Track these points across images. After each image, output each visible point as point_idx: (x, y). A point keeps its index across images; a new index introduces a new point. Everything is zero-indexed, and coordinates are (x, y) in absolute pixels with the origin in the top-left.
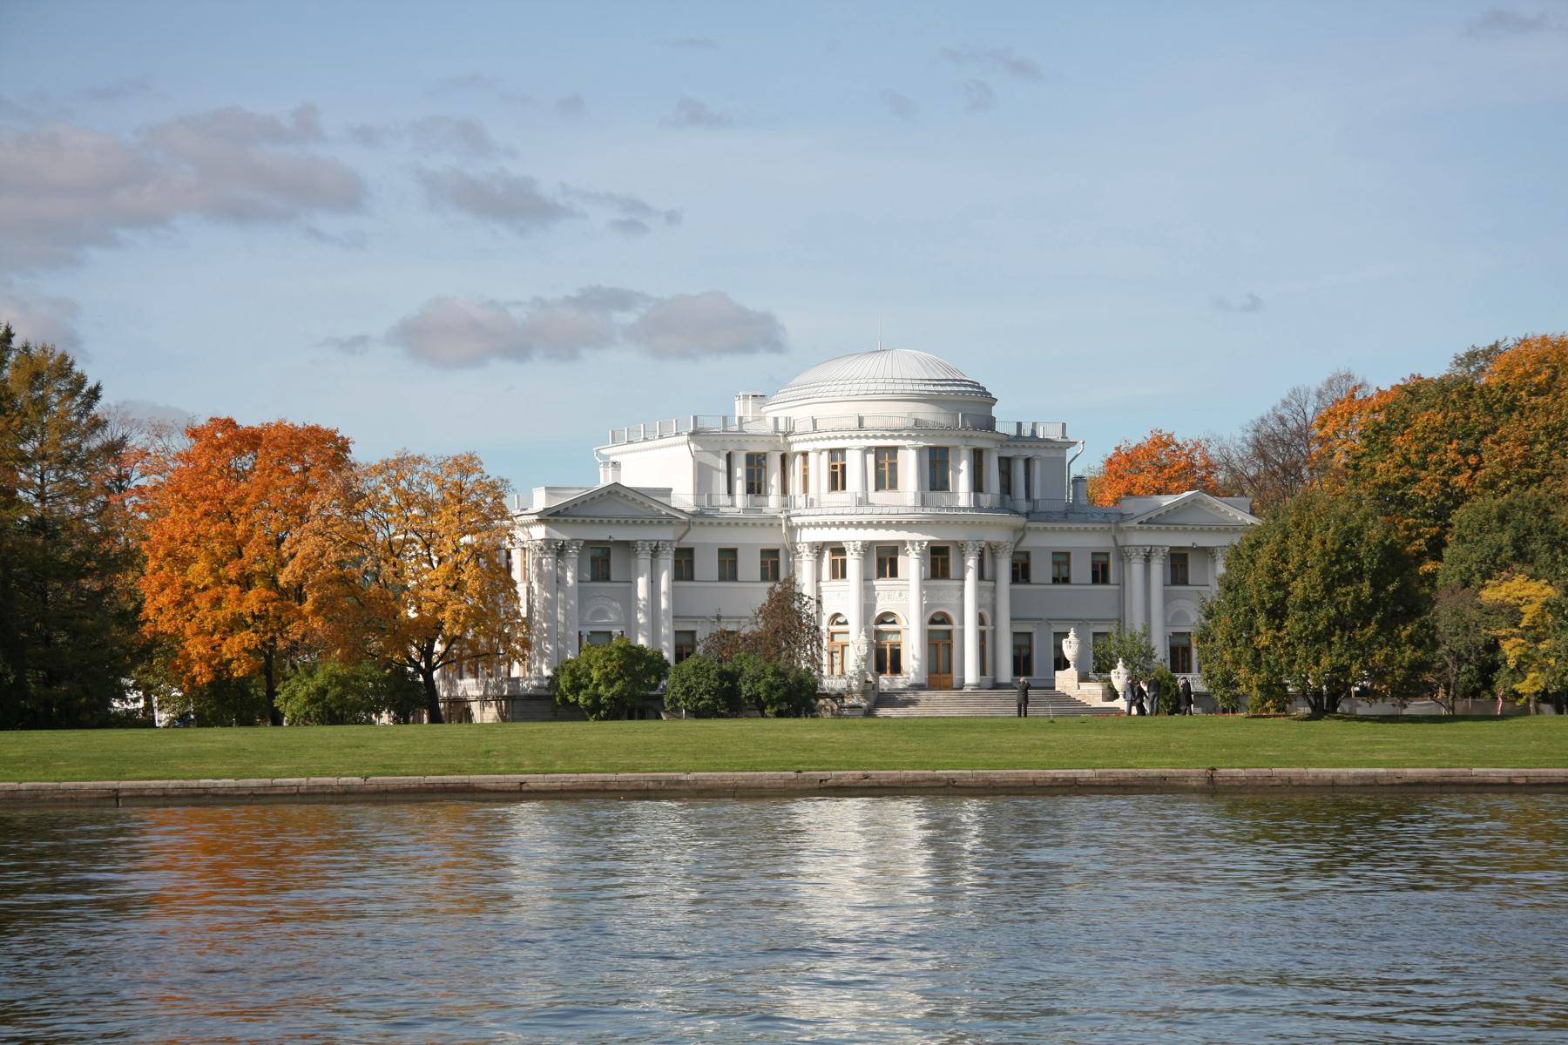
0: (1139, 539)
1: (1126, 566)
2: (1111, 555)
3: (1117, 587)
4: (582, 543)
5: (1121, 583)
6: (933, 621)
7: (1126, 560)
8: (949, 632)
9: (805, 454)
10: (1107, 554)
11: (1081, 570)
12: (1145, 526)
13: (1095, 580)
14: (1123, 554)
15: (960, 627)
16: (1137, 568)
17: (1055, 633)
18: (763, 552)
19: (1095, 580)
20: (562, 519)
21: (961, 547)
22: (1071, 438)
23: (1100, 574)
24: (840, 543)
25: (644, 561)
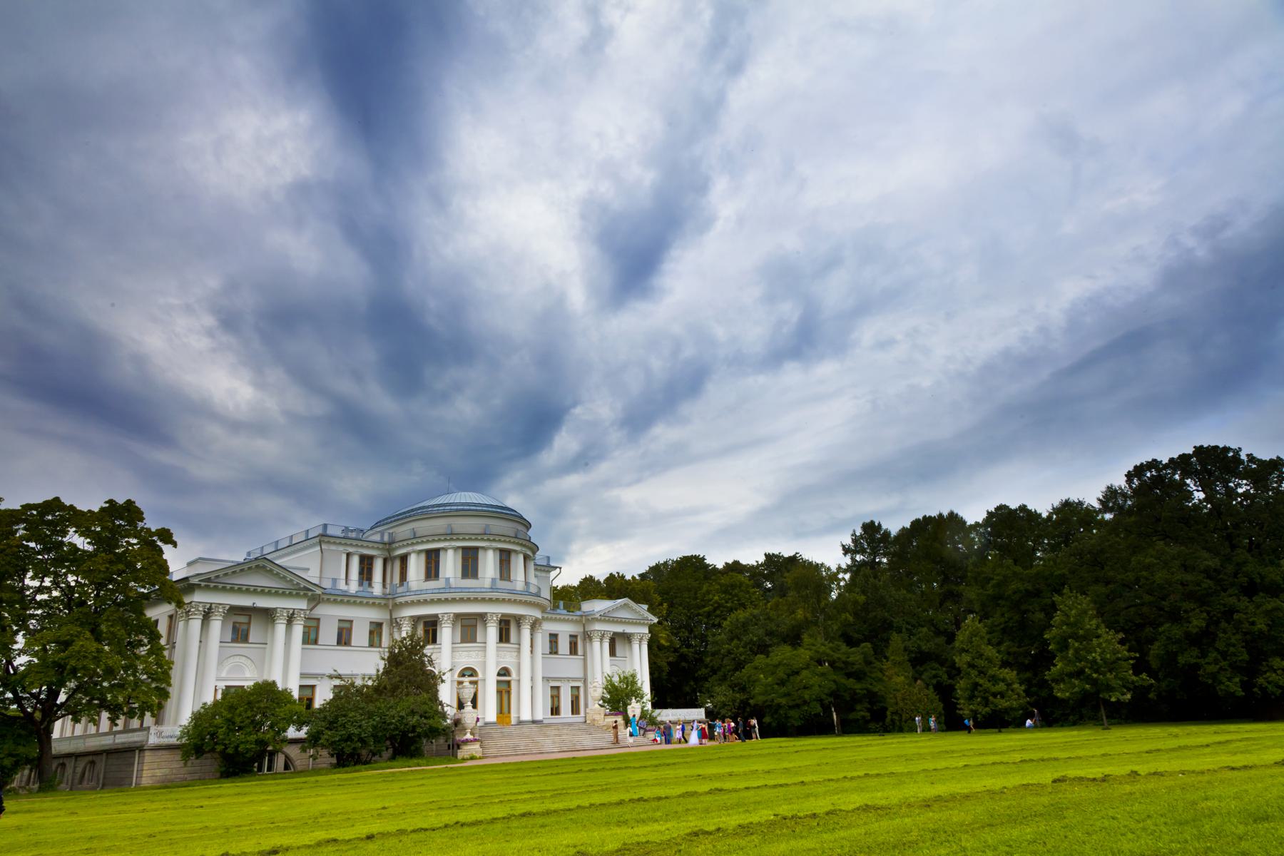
0: (598, 627)
1: (588, 644)
2: (579, 637)
3: (582, 657)
4: (227, 607)
5: (585, 655)
6: (499, 674)
7: (588, 640)
8: (509, 683)
9: (404, 559)
10: (575, 637)
11: (564, 645)
12: (603, 618)
13: (571, 653)
14: (588, 637)
15: (517, 678)
16: (596, 644)
17: (551, 687)
18: (371, 622)
19: (571, 653)
20: (212, 585)
21: (518, 620)
22: (552, 564)
23: (573, 650)
24: (436, 616)
25: (281, 628)
